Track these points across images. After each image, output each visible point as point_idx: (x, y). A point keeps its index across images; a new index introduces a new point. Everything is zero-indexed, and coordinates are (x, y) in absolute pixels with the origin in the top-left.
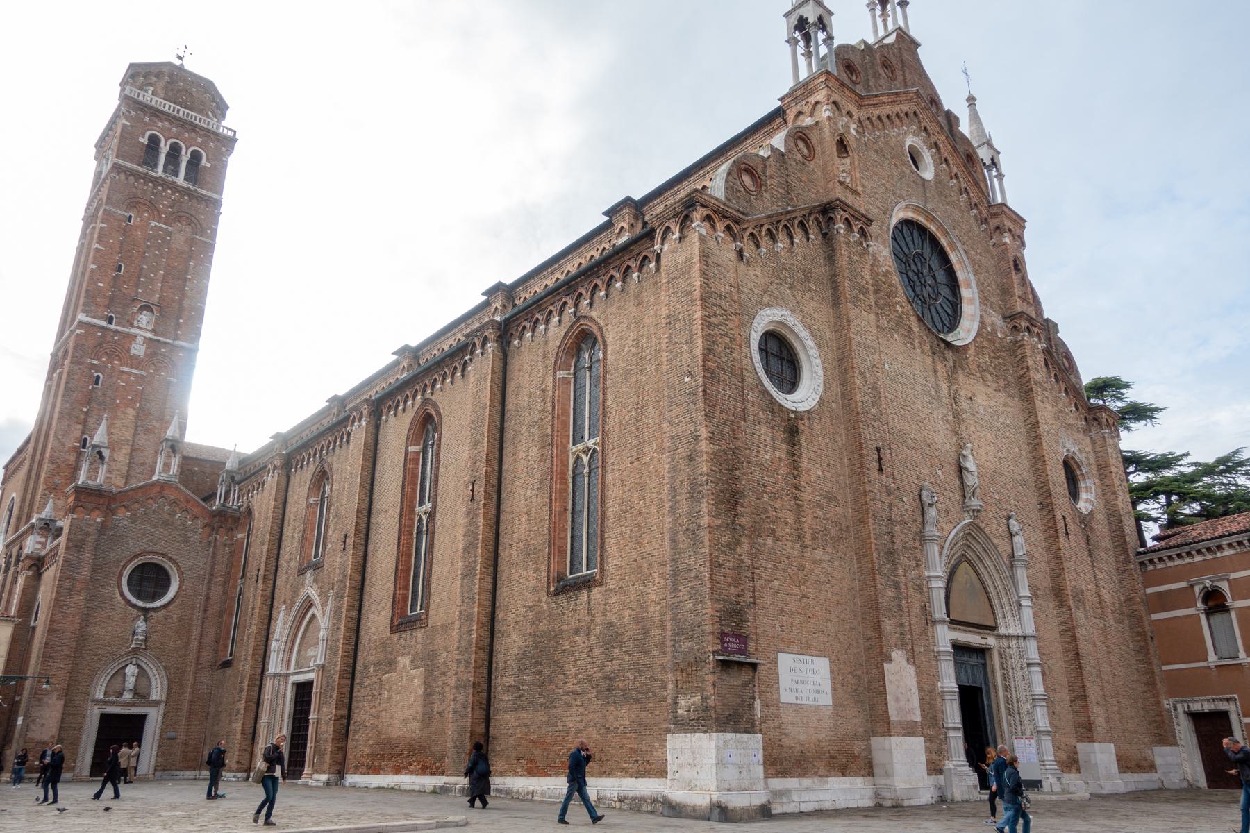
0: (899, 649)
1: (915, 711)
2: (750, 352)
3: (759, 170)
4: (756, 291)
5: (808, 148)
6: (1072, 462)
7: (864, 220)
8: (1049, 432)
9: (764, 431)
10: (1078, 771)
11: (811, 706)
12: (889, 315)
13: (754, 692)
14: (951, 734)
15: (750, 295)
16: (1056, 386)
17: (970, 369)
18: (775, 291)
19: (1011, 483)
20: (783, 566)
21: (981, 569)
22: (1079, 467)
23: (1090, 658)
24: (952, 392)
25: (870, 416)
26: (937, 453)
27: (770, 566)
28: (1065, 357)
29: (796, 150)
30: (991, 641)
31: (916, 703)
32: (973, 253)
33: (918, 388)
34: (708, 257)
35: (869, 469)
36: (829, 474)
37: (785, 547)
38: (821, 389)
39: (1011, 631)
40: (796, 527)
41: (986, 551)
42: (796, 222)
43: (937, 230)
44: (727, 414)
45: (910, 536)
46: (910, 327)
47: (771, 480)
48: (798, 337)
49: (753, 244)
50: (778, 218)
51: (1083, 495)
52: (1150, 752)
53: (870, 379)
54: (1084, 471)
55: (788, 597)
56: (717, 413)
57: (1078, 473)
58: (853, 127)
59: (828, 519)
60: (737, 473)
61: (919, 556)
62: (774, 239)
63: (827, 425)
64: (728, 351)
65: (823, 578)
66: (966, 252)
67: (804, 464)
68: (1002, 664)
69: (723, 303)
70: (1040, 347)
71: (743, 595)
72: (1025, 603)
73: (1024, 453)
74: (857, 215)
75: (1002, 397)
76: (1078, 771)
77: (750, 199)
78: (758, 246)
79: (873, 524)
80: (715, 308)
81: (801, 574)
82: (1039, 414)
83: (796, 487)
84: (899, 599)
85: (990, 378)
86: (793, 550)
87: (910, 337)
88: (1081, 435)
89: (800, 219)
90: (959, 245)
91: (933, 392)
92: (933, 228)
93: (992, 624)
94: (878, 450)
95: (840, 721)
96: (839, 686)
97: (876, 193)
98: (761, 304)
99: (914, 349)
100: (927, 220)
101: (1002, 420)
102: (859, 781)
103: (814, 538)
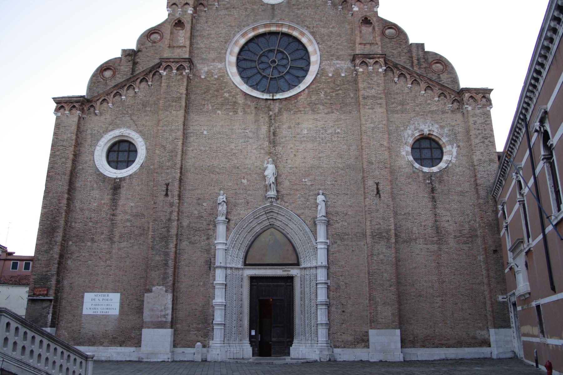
0: (159, 286)
1: (167, 317)
2: (94, 158)
3: (116, 65)
4: (104, 126)
5: (160, 36)
6: (433, 137)
7: (183, 60)
8: (373, 129)
9: (96, 194)
10: (368, 347)
11: (103, 315)
12: (215, 102)
13: (49, 311)
14: (215, 327)
15: (99, 130)
16: (416, 88)
17: (298, 108)
18: (118, 122)
19: (331, 171)
20: (96, 253)
21: (287, 230)
22: (440, 139)
23: (385, 275)
24: (272, 128)
25: (164, 168)
26: (246, 170)
27: (87, 255)
28: (437, 63)
29: (148, 42)
30: (294, 272)
31: (169, 312)
32: (323, 29)
33: (234, 136)
34: (59, 125)
35: (156, 197)
36: (139, 203)
37: (99, 245)
38: (142, 162)
39: (309, 265)
40: (108, 234)
41: (288, 219)
42: (139, 80)
43: (289, 29)
44: (57, 193)
45: (205, 223)
46: (235, 103)
47: (97, 215)
48: (131, 138)
49: (106, 103)
50: (124, 84)
51: (445, 158)
52: (483, 333)
53: (169, 147)
54: (444, 141)
55: (97, 268)
56: (51, 195)
57: (441, 143)
58: (190, 11)
59: (134, 226)
60: (58, 218)
61: (211, 232)
62: (121, 95)
63: (144, 179)
64: (63, 165)
65: (124, 255)
66: (313, 33)
67: (121, 202)
68: (301, 285)
69: (65, 144)
70: (380, 70)
71: (50, 271)
72: (319, 246)
73: (354, 147)
74: (176, 60)
75: (334, 116)
76: (368, 347)
77: (106, 82)
78: (108, 103)
79: (153, 225)
80: (59, 147)
81: (108, 256)
82: (363, 119)
83: (113, 215)
84: (167, 261)
85: (321, 107)
86: (104, 246)
87: (234, 108)
88: (446, 115)
89: (142, 78)
90: (306, 32)
91: (250, 135)
92: (285, 30)
93: (296, 262)
94: (167, 185)
95: (123, 322)
96: (126, 305)
97: (219, 34)
98: (107, 131)
99: (237, 114)
100: (279, 27)
101: (329, 131)
102: (132, 349)
103: (121, 237)
